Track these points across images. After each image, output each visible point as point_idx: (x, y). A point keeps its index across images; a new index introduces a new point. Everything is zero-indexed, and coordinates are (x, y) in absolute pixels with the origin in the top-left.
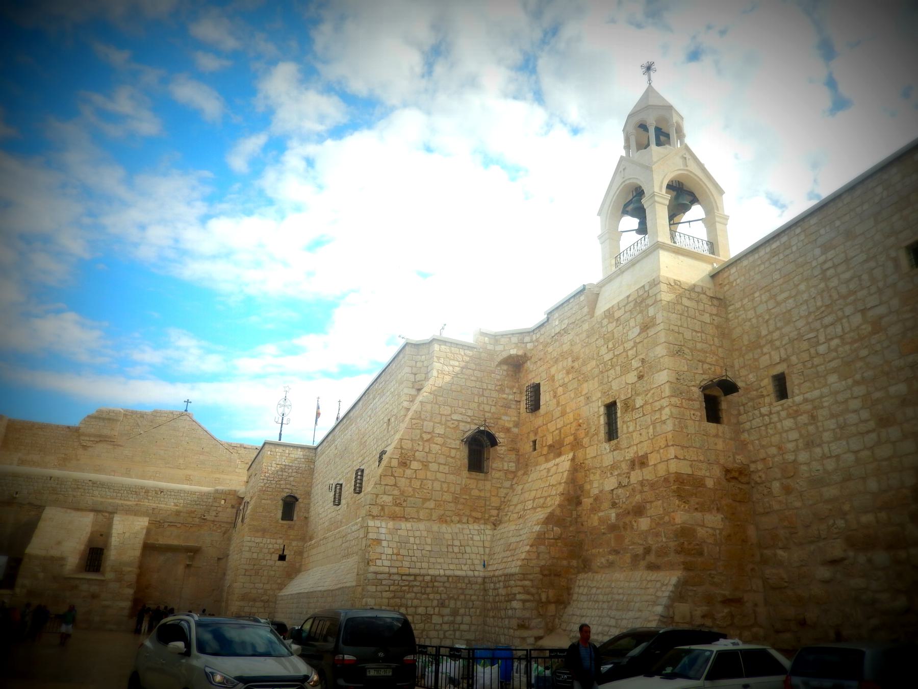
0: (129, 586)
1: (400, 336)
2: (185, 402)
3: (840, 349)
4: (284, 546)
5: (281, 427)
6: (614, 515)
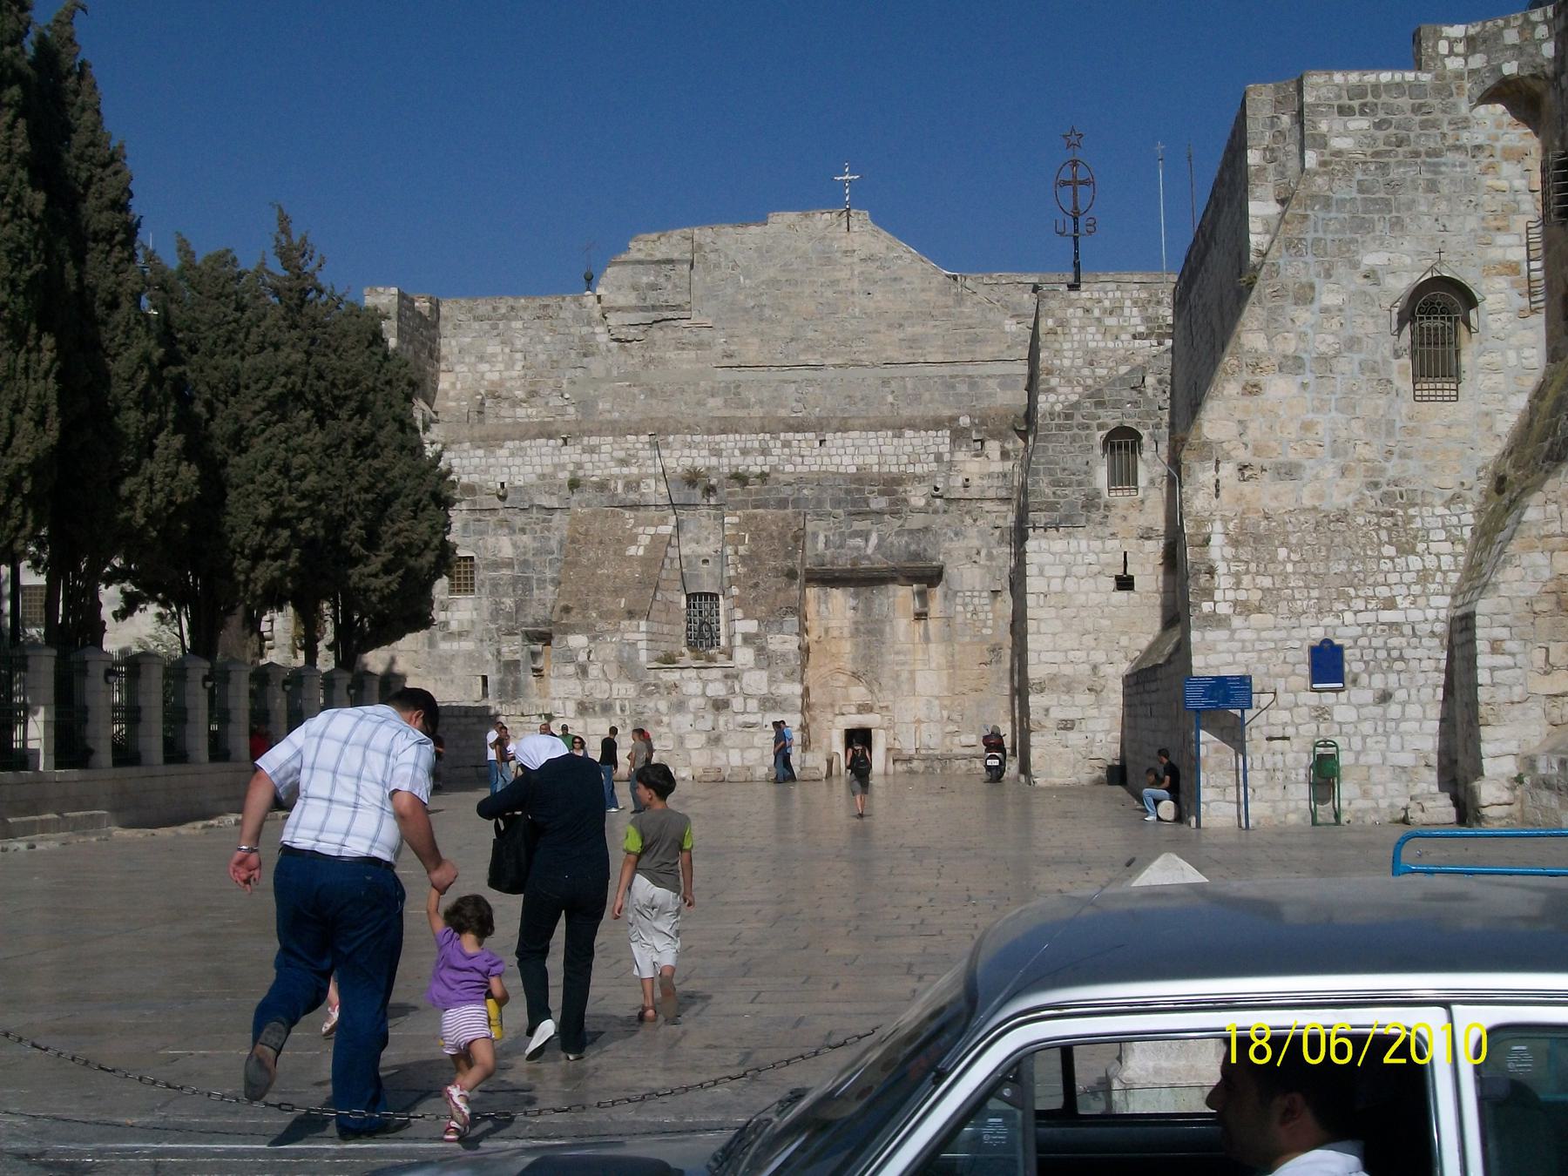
0: (789, 676)
4: (1125, 553)
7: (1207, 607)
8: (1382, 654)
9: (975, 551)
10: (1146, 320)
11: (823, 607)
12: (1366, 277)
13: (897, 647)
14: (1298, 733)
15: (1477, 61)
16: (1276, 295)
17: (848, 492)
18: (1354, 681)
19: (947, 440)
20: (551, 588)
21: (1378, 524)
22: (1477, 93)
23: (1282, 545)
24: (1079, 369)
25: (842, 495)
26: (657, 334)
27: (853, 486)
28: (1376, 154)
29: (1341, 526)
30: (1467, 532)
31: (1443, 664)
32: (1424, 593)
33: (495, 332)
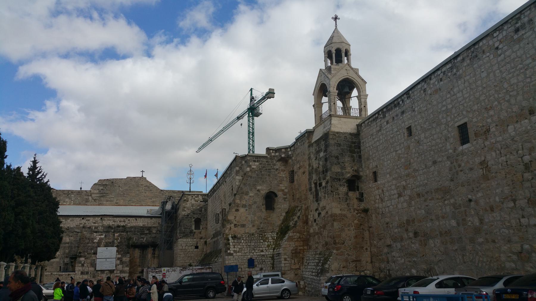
0: (127, 266)
1: (234, 153)
2: (141, 172)
3: (390, 165)
5: (190, 185)
6: (317, 228)
7: (229, 251)
8: (261, 261)
10: (203, 199)
11: (134, 252)
12: (258, 191)
14: (245, 276)
15: (277, 154)
16: (243, 193)
17: (140, 230)
18: (256, 266)
19: (161, 220)
20: (77, 248)
21: (259, 236)
22: (277, 160)
23: (242, 240)
24: (190, 207)
26: (102, 199)
28: (260, 169)
29: (253, 236)
30: (275, 238)
31: (272, 263)
32: (268, 249)
33: (68, 197)
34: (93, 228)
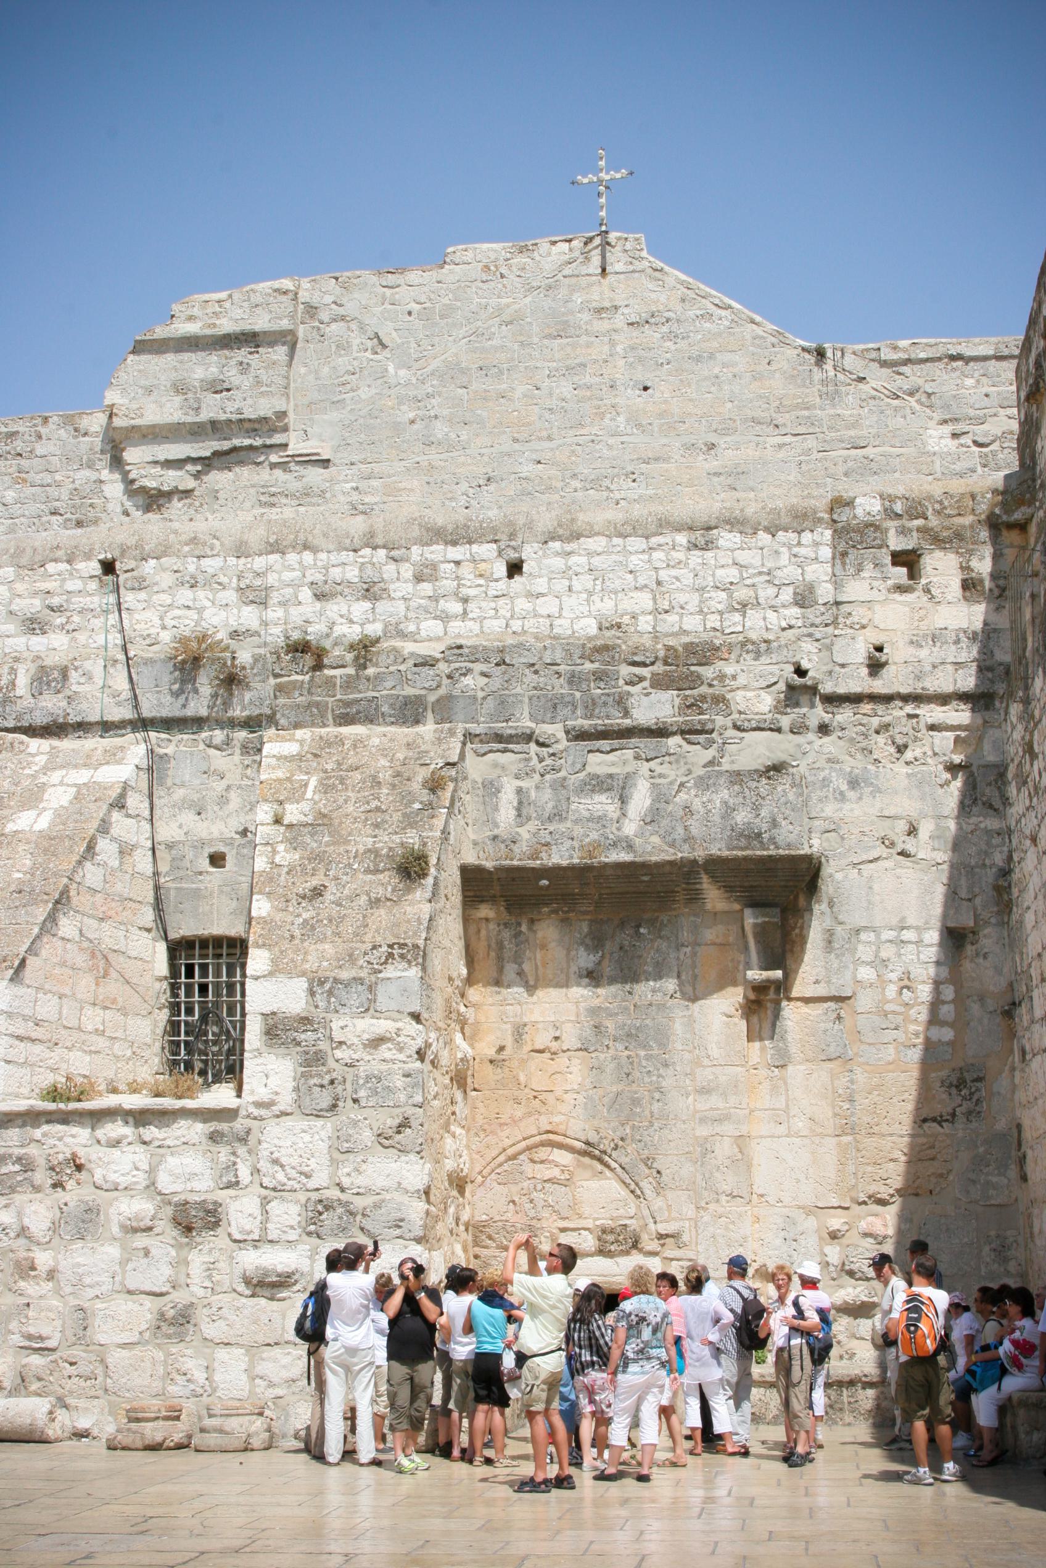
9: (902, 826)
13: (705, 1075)
17: (573, 680)
19: (826, 552)
25: (561, 687)
26: (218, 478)
27: (588, 666)
34: (23, 682)
